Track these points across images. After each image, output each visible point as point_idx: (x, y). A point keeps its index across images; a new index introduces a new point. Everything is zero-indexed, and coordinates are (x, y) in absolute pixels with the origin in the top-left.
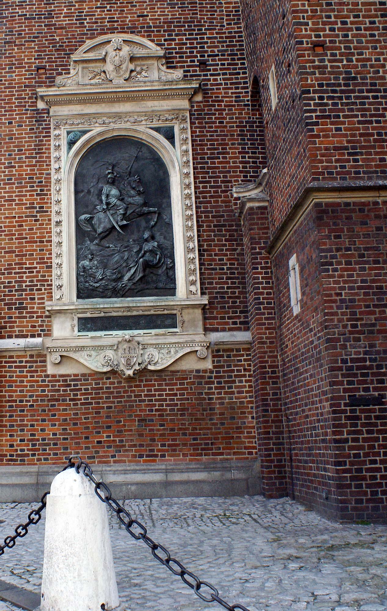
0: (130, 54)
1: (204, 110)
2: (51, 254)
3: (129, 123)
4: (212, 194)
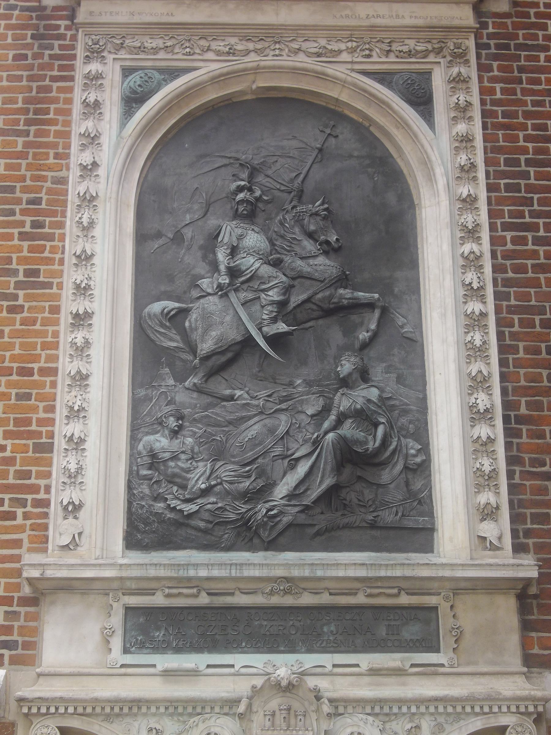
2: (51, 409)
3: (301, 57)
4: (542, 260)
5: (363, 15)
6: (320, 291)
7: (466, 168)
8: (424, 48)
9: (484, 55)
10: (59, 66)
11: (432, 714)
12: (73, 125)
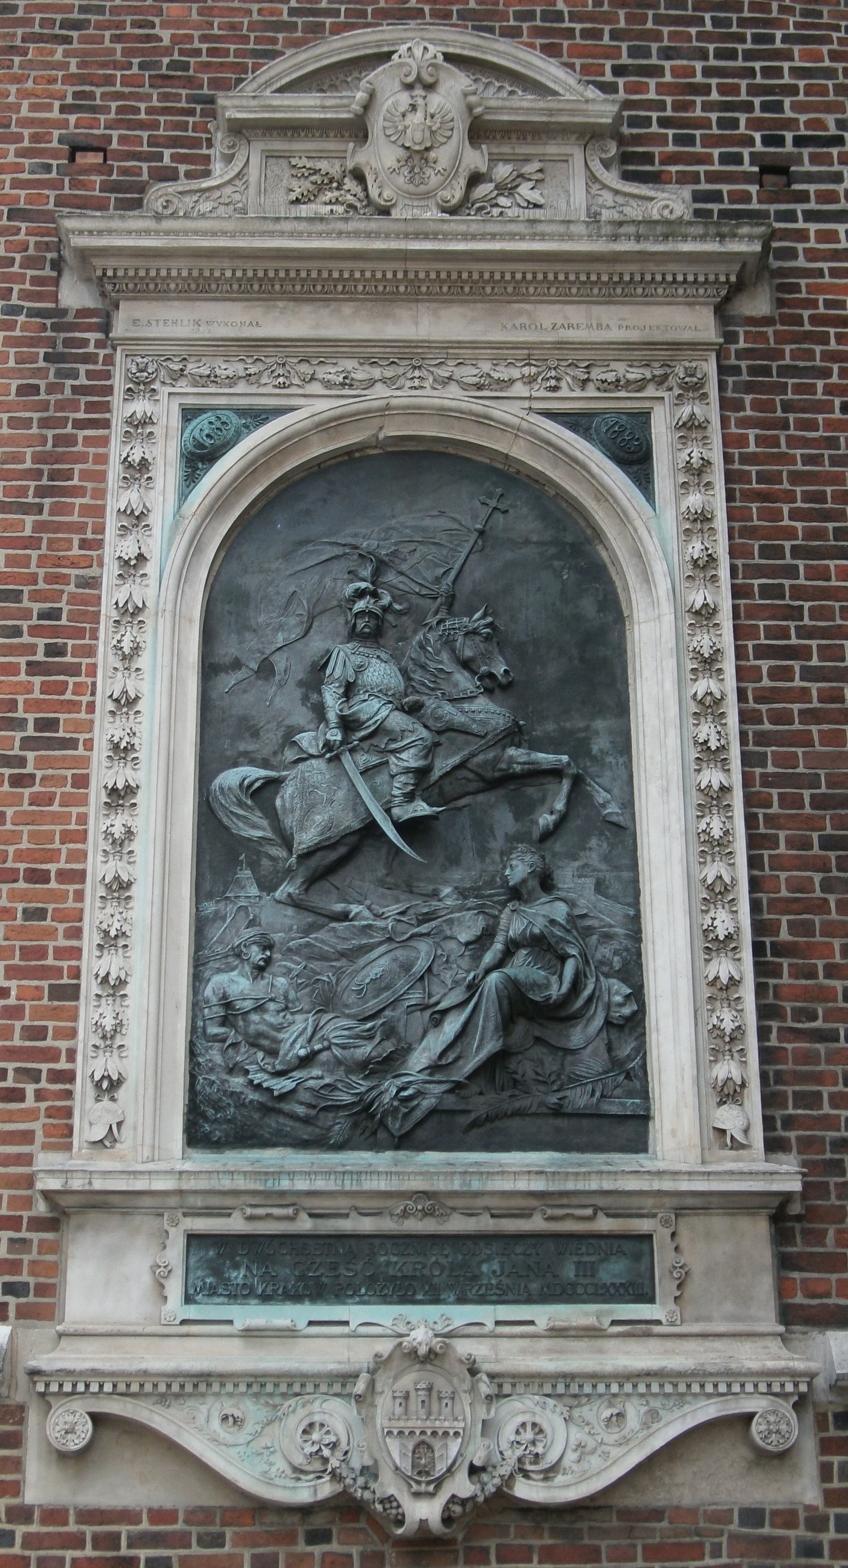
0: (470, 108)
1: (781, 355)
2: (76, 933)
3: (454, 390)
4: (815, 704)
5: (547, 324)
7: (700, 562)
8: (639, 377)
9: (730, 385)
10: (87, 403)
11: (642, 1395)
12: (109, 497)
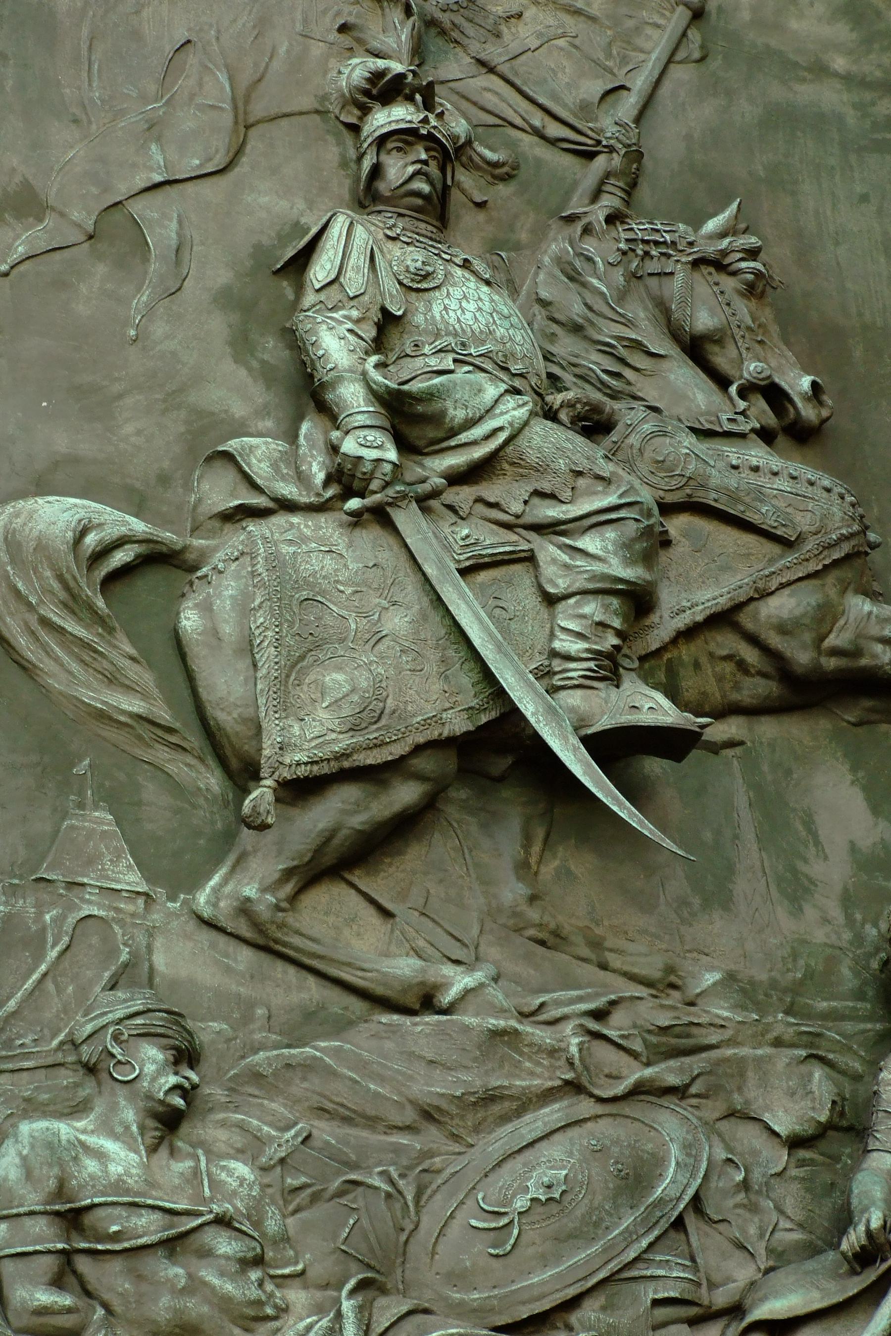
6: (782, 586)
